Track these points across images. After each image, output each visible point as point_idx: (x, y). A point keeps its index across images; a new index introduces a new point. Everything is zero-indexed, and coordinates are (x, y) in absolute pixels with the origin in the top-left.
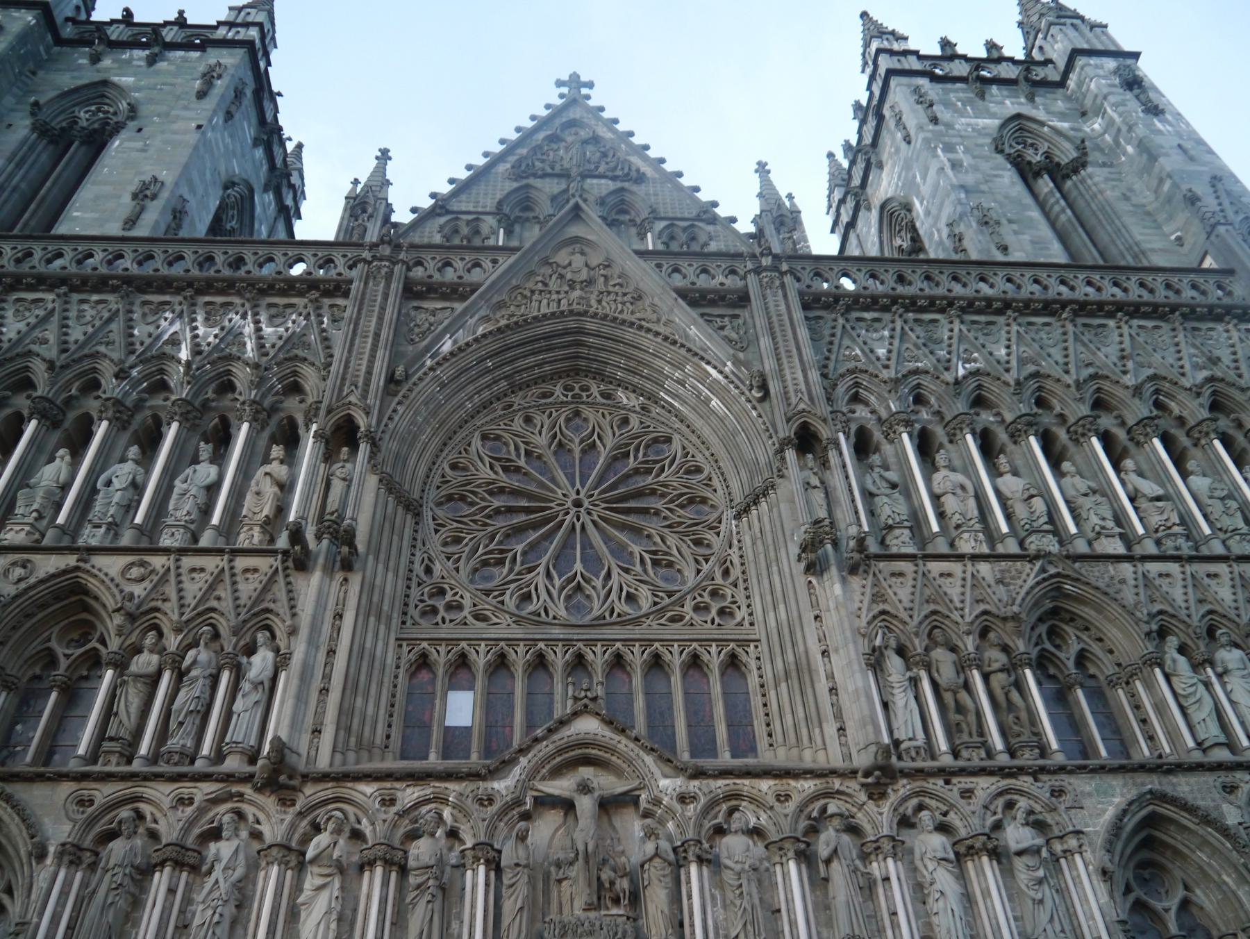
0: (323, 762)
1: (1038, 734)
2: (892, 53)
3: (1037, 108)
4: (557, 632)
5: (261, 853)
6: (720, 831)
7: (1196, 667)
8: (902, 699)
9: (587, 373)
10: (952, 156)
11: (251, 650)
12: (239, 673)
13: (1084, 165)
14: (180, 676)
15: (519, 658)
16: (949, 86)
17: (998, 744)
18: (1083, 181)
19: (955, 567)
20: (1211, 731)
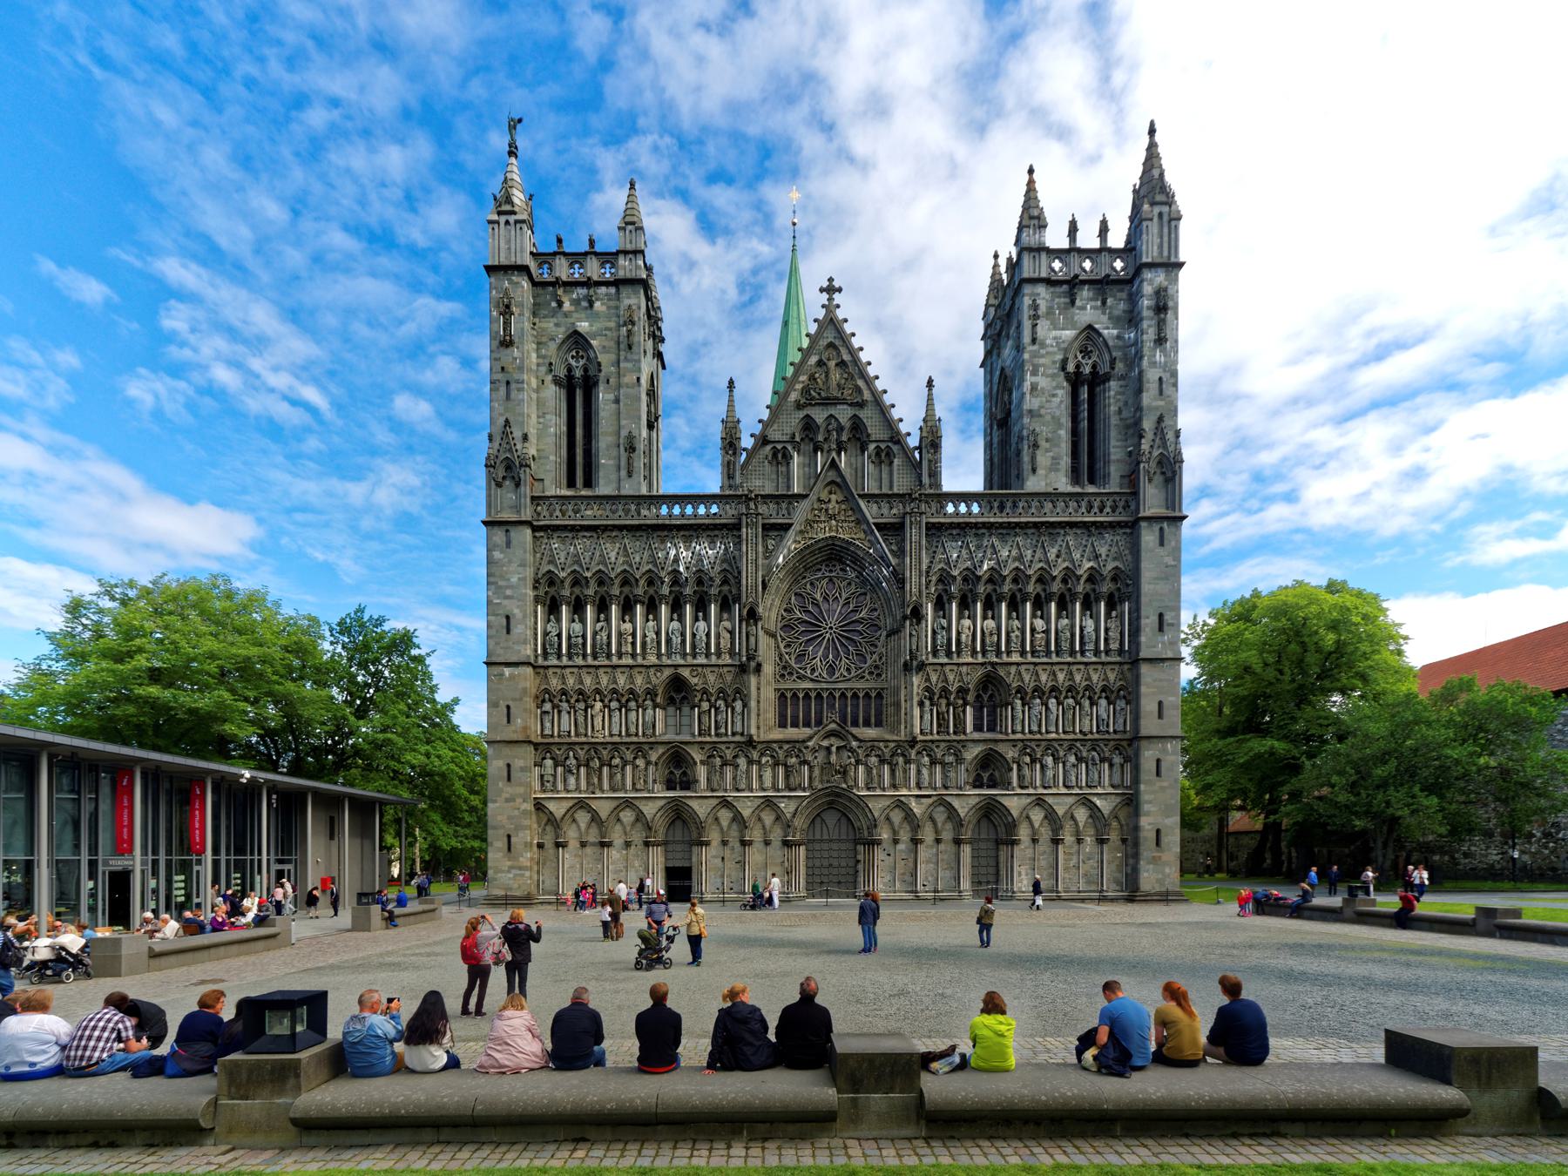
0: (762, 739)
1: (965, 728)
2: (1030, 250)
3: (1104, 313)
4: (825, 686)
5: (750, 762)
6: (867, 755)
7: (1023, 705)
8: (927, 716)
9: (835, 559)
10: (1034, 379)
11: (734, 700)
12: (733, 709)
13: (1109, 380)
14: (717, 709)
15: (813, 695)
16: (1059, 290)
17: (951, 731)
18: (1104, 391)
19: (955, 668)
20: (1019, 728)
